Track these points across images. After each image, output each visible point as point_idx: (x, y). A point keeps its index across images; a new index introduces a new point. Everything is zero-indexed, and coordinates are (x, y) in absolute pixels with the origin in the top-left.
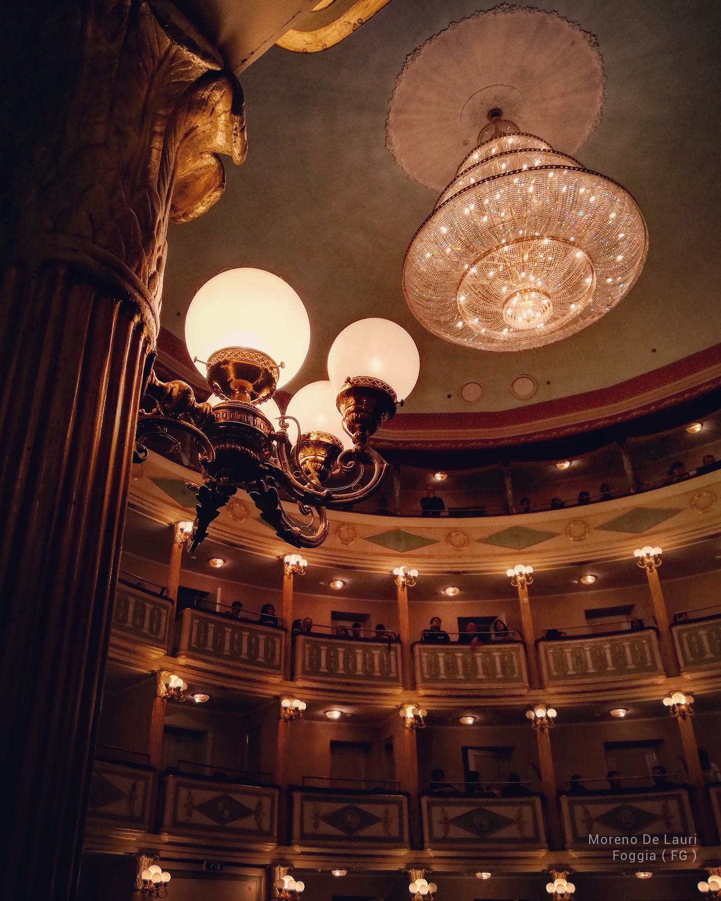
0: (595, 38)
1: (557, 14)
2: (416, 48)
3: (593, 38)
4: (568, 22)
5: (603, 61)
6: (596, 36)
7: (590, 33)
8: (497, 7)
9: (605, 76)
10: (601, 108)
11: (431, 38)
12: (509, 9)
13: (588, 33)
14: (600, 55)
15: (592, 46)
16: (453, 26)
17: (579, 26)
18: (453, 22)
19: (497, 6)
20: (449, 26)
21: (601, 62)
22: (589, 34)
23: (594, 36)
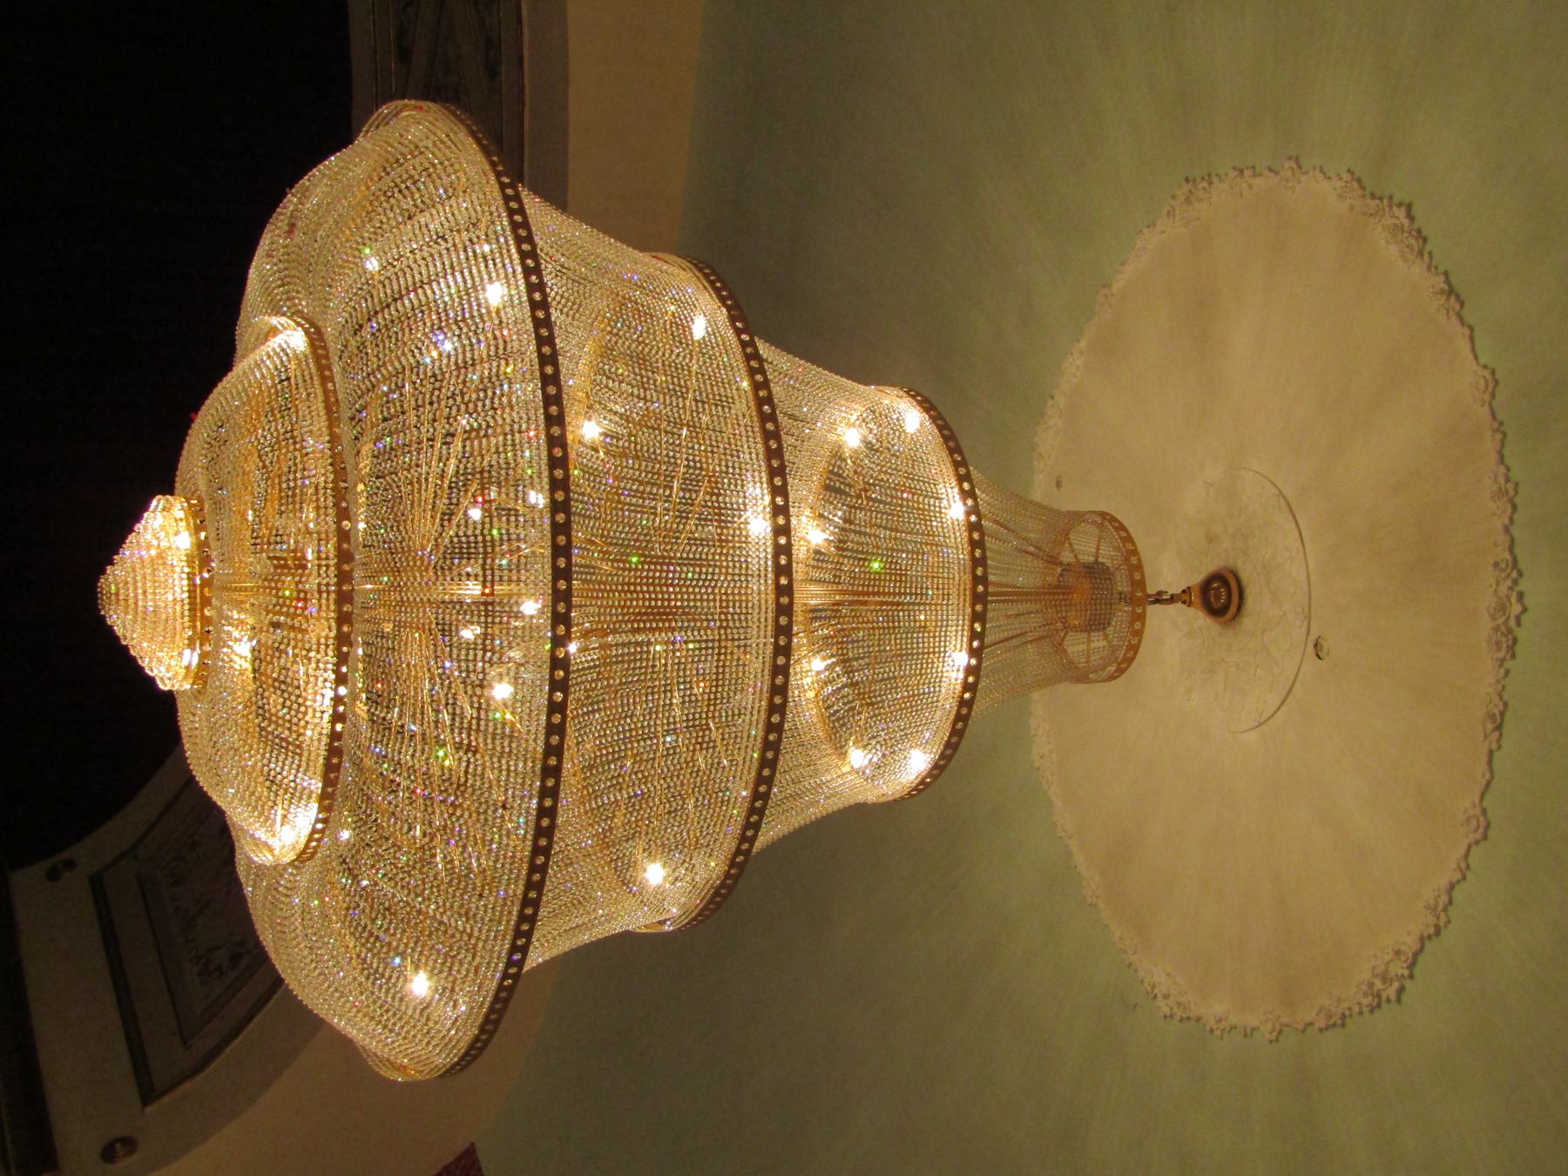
0: (1393, 998)
1: (1477, 842)
2: (1425, 240)
3: (1391, 992)
4: (1452, 887)
5: (1327, 1028)
6: (1399, 1000)
7: (1411, 976)
8: (1514, 575)
9: (1280, 1032)
10: (1198, 1019)
11: (1451, 292)
12: (1503, 629)
13: (1412, 966)
14: (1343, 1017)
15: (1371, 985)
16: (1482, 383)
17: (1432, 931)
18: (1497, 382)
19: (1520, 574)
20: (1485, 367)
21: (1321, 1023)
22: (1406, 972)
23: (1401, 990)
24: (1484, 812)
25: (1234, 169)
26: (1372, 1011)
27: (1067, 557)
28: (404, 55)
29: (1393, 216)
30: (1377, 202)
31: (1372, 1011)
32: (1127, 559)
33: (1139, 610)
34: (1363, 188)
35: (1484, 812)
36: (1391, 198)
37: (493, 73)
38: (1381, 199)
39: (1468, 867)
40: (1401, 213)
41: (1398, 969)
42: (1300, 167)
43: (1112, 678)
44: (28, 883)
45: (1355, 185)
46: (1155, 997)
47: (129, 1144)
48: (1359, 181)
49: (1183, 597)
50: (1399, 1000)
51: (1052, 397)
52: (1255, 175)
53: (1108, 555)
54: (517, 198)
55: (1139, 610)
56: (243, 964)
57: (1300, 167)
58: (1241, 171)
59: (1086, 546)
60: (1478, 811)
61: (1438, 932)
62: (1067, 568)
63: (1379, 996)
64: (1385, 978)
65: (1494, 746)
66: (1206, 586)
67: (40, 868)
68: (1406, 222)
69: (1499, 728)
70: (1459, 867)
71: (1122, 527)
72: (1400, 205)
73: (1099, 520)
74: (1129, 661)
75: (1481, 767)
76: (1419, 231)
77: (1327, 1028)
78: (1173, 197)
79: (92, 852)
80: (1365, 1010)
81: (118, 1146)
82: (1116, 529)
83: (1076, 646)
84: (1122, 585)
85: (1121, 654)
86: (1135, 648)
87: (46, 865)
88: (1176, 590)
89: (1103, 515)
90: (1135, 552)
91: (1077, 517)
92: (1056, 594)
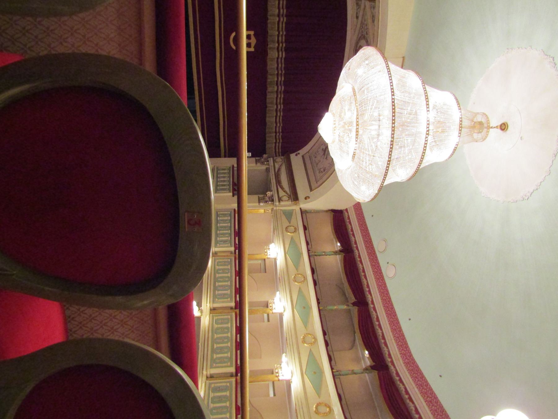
0: (526, 199)
1: (547, 175)
2: (556, 65)
3: (526, 198)
4: (541, 182)
5: (513, 202)
6: (527, 199)
7: (531, 196)
9: (504, 202)
14: (516, 201)
15: (522, 197)
17: (536, 189)
22: (530, 195)
24: (550, 170)
25: (518, 47)
26: (522, 201)
27: (475, 120)
28: (357, 17)
29: (550, 60)
30: (547, 56)
31: (522, 201)
32: (487, 122)
33: (488, 130)
34: (544, 53)
35: (550, 170)
36: (550, 56)
37: (373, 21)
38: (548, 56)
39: (545, 179)
40: (552, 59)
41: (529, 194)
42: (531, 48)
43: (482, 141)
44: (293, 156)
45: (543, 53)
46: (481, 193)
47: (309, 197)
48: (544, 52)
49: (497, 127)
50: (527, 199)
51: (475, 88)
52: (522, 49)
53: (484, 120)
54: (388, 64)
55: (488, 130)
56: (326, 171)
57: (531, 48)
58: (519, 48)
59: (479, 119)
60: (549, 170)
61: (537, 189)
62: (475, 123)
63: (524, 199)
64: (525, 196)
65: (554, 159)
66: (501, 125)
67: (294, 154)
68: (552, 61)
69: (555, 156)
70: (543, 179)
71: (487, 116)
72: (552, 57)
73: (482, 114)
74: (485, 139)
75: (551, 162)
76: (555, 63)
77: (513, 202)
78: (504, 52)
79: (302, 151)
80: (521, 201)
81: (307, 197)
82: (486, 116)
83: (475, 136)
84: (485, 125)
85: (484, 138)
86: (486, 137)
87: (296, 153)
88: (495, 126)
89: (483, 113)
90: (489, 120)
91: (478, 113)
92: (473, 127)
